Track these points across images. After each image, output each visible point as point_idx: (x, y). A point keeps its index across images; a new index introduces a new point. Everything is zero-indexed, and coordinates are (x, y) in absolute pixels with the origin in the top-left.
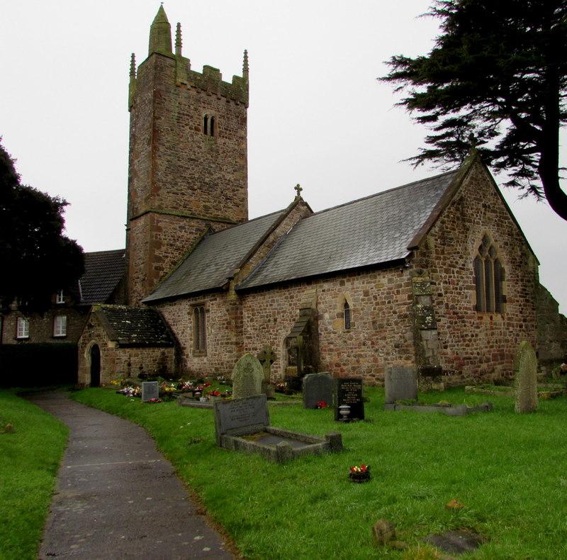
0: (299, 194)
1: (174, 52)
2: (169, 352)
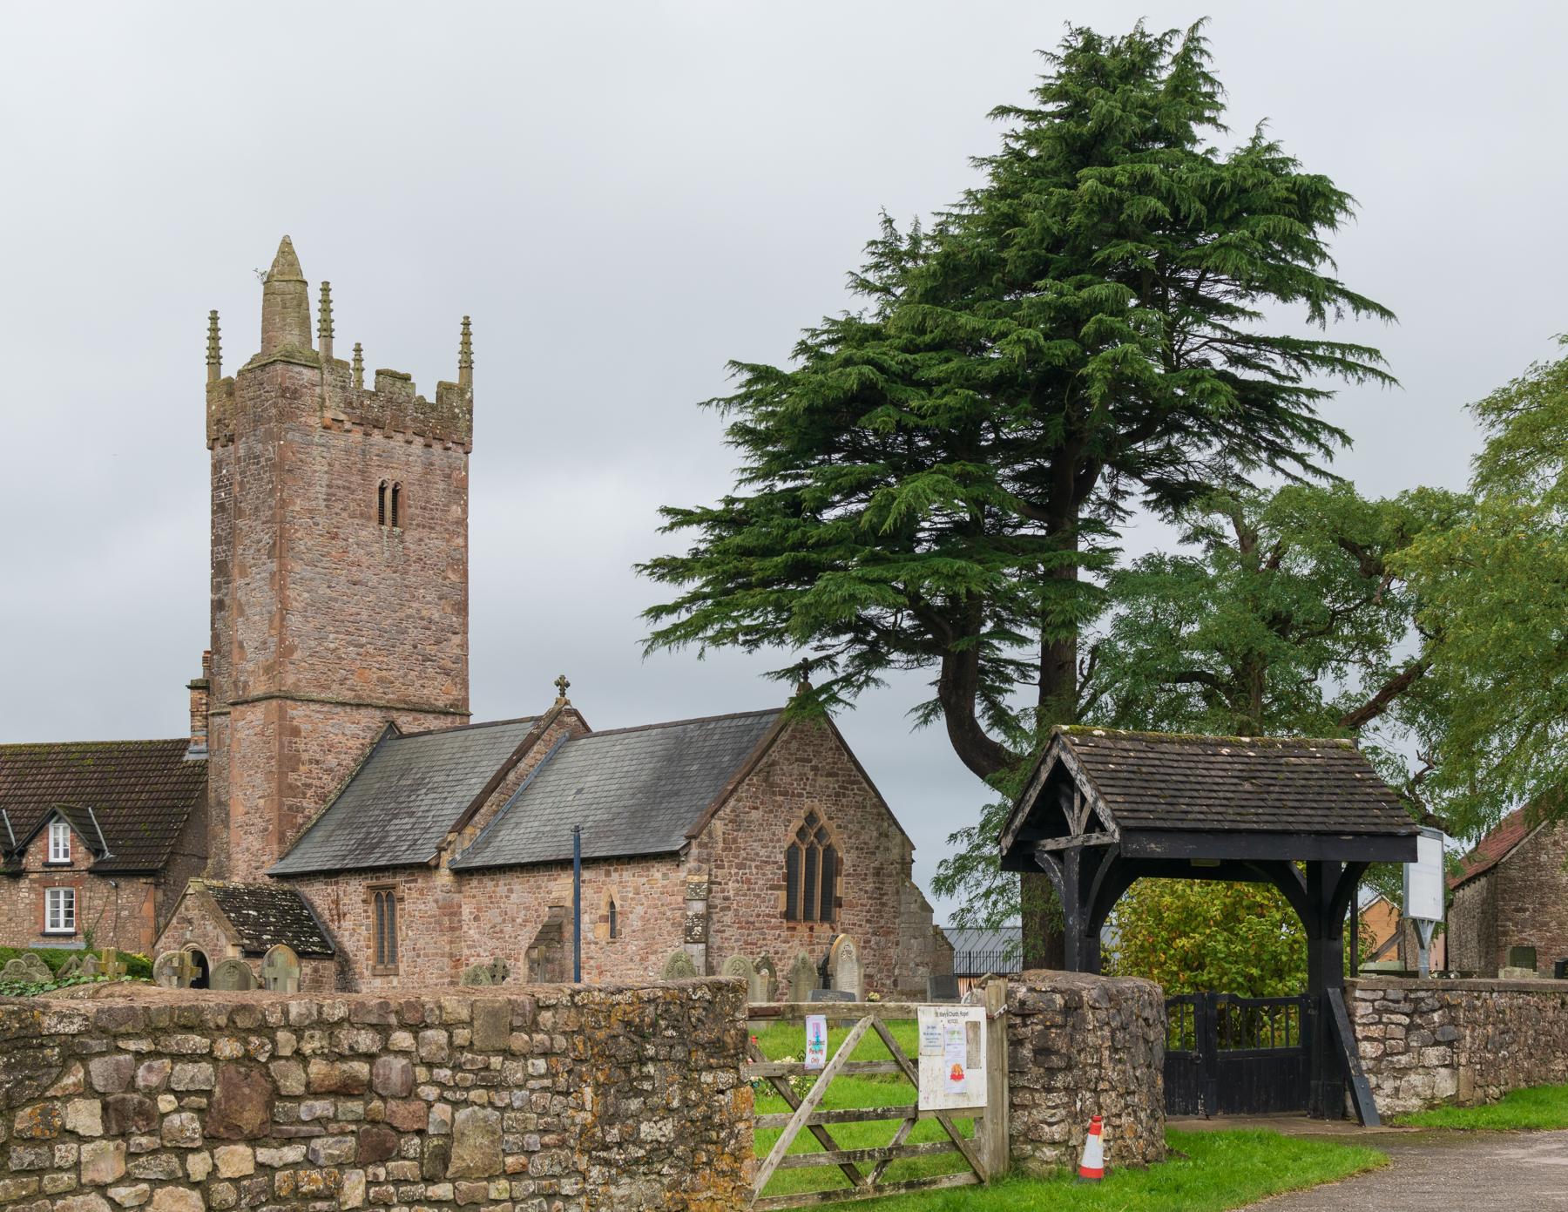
0: (563, 694)
1: (316, 345)
2: (325, 968)
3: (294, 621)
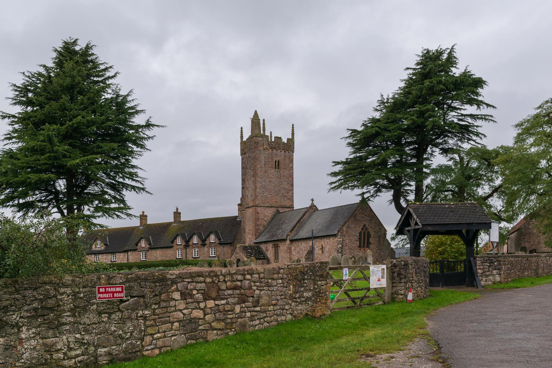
3: (258, 190)
